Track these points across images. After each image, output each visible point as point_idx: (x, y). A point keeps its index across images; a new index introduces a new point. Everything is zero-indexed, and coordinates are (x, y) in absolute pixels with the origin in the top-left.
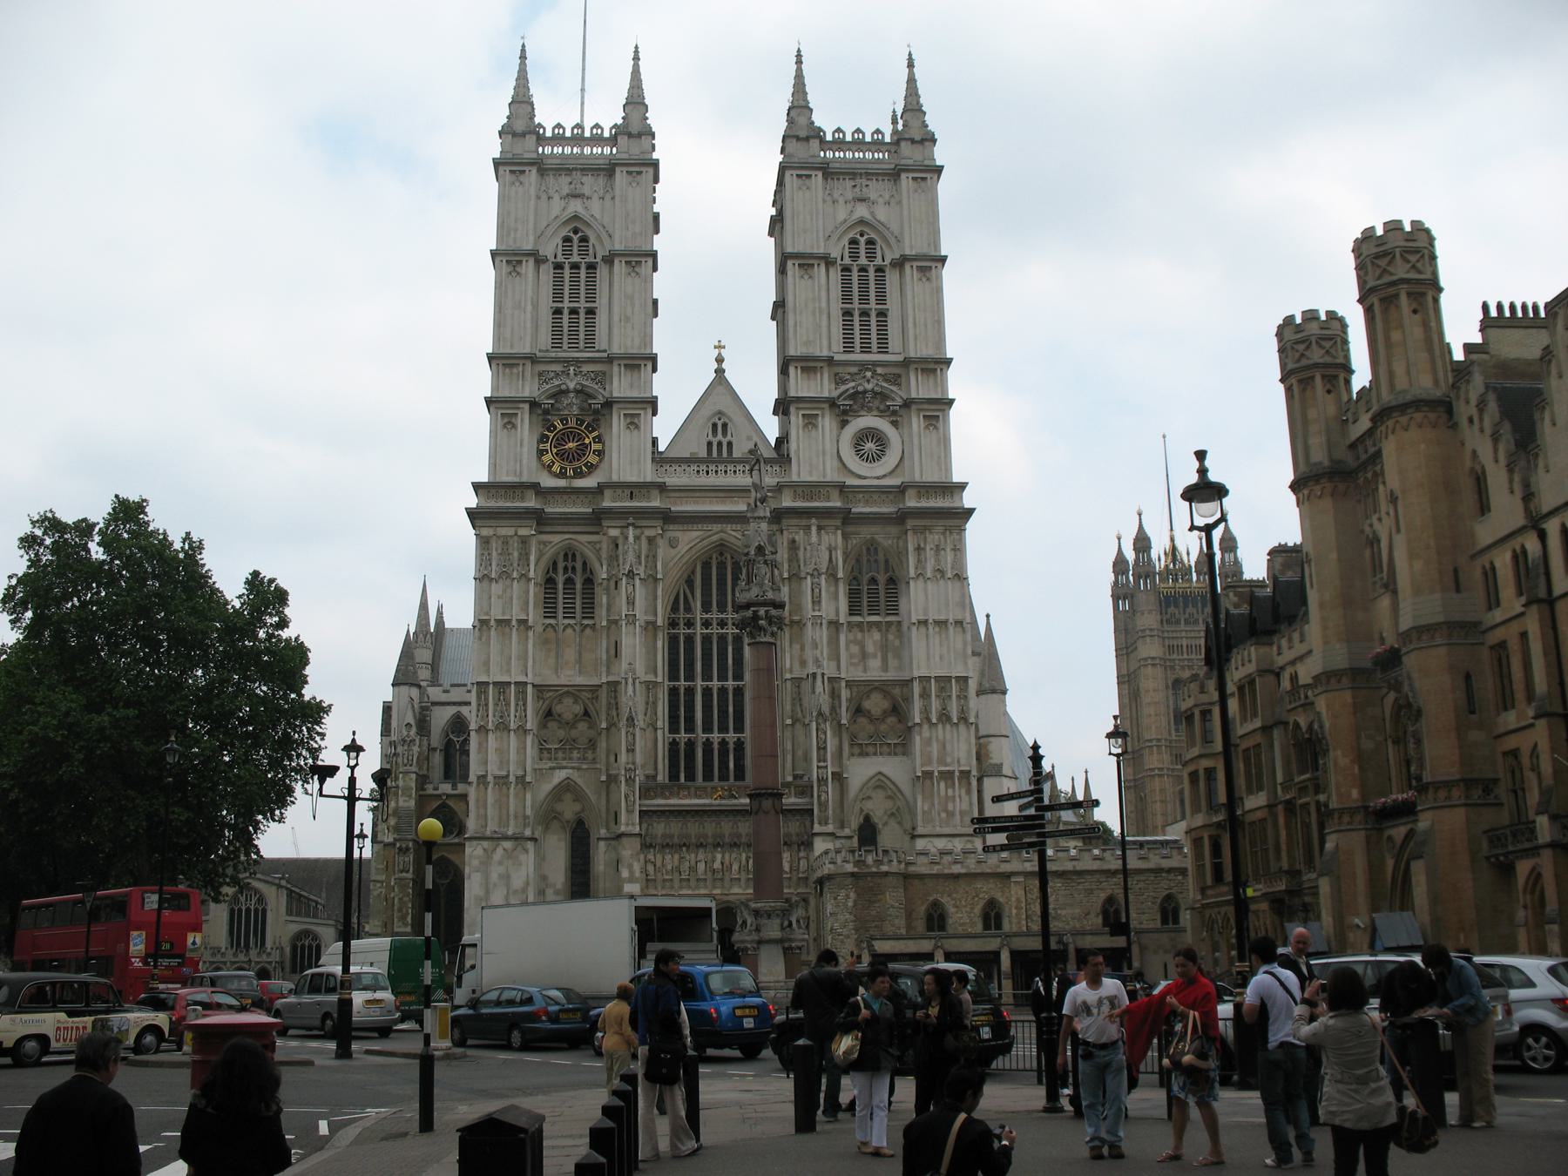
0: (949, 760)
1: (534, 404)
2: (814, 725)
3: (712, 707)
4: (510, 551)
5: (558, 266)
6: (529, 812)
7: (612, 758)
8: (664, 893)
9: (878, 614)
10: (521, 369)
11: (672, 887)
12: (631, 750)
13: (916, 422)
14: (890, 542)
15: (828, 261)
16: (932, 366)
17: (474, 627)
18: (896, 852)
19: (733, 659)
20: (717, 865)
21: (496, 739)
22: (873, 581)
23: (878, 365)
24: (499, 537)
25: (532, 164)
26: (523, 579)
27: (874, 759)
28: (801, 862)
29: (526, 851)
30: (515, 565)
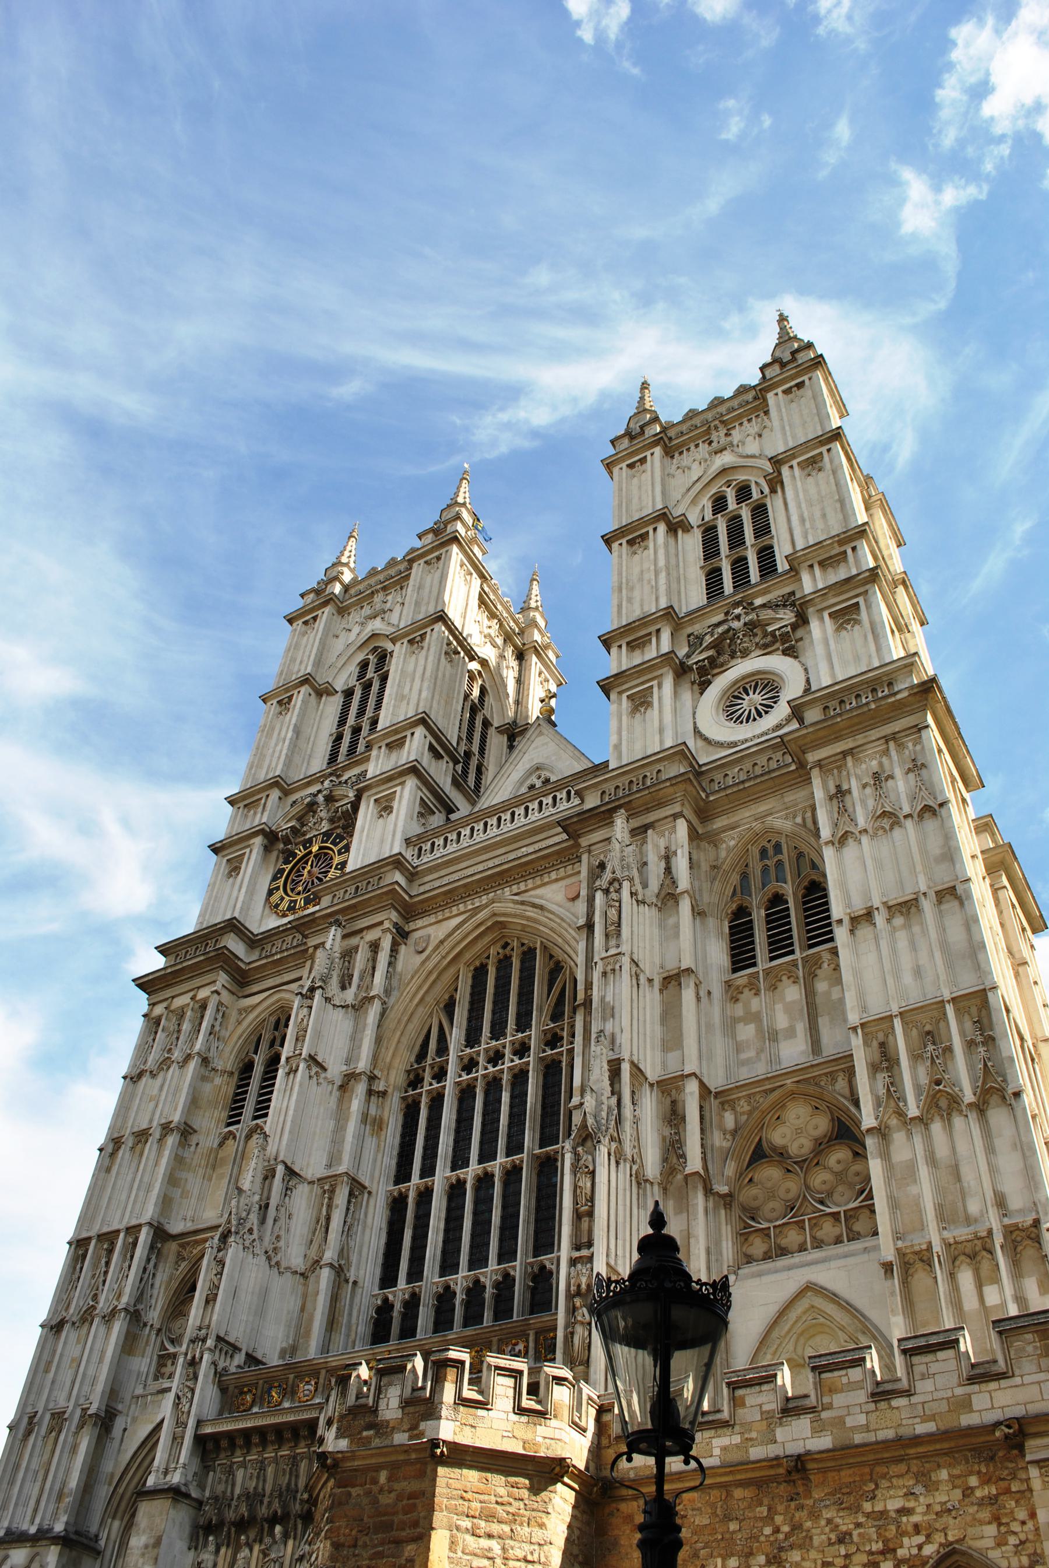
0: (973, 1207)
1: (271, 837)
5: (349, 693)
9: (792, 952)
10: (263, 801)
13: (820, 629)
14: (799, 820)
15: (676, 526)
16: (837, 550)
17: (101, 1150)
18: (516, 1374)
21: (78, 1342)
22: (777, 899)
23: (756, 597)
24: (172, 1011)
25: (325, 604)
27: (797, 1258)
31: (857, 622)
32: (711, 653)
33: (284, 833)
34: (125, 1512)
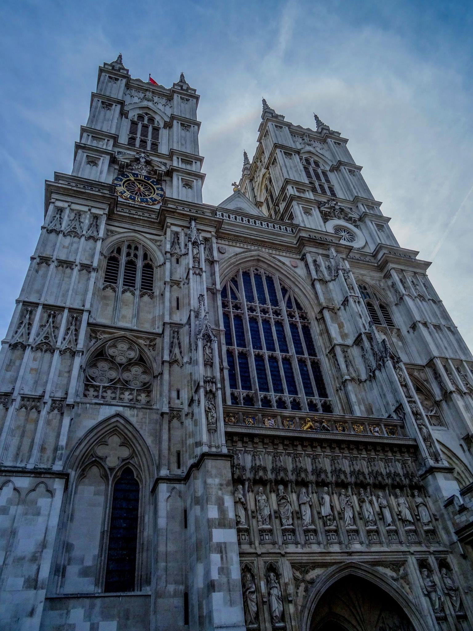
2: (389, 363)
3: (265, 370)
4: (82, 220)
6: (63, 441)
7: (174, 394)
8: (264, 551)
9: (381, 324)
11: (274, 543)
12: (209, 364)
17: (32, 259)
19: (278, 337)
20: (326, 510)
21: (35, 359)
24: (72, 210)
26: (91, 242)
28: (420, 509)
29: (51, 493)
30: (85, 228)
31: (383, 231)
32: (329, 210)
33: (123, 163)
34: (77, 467)
